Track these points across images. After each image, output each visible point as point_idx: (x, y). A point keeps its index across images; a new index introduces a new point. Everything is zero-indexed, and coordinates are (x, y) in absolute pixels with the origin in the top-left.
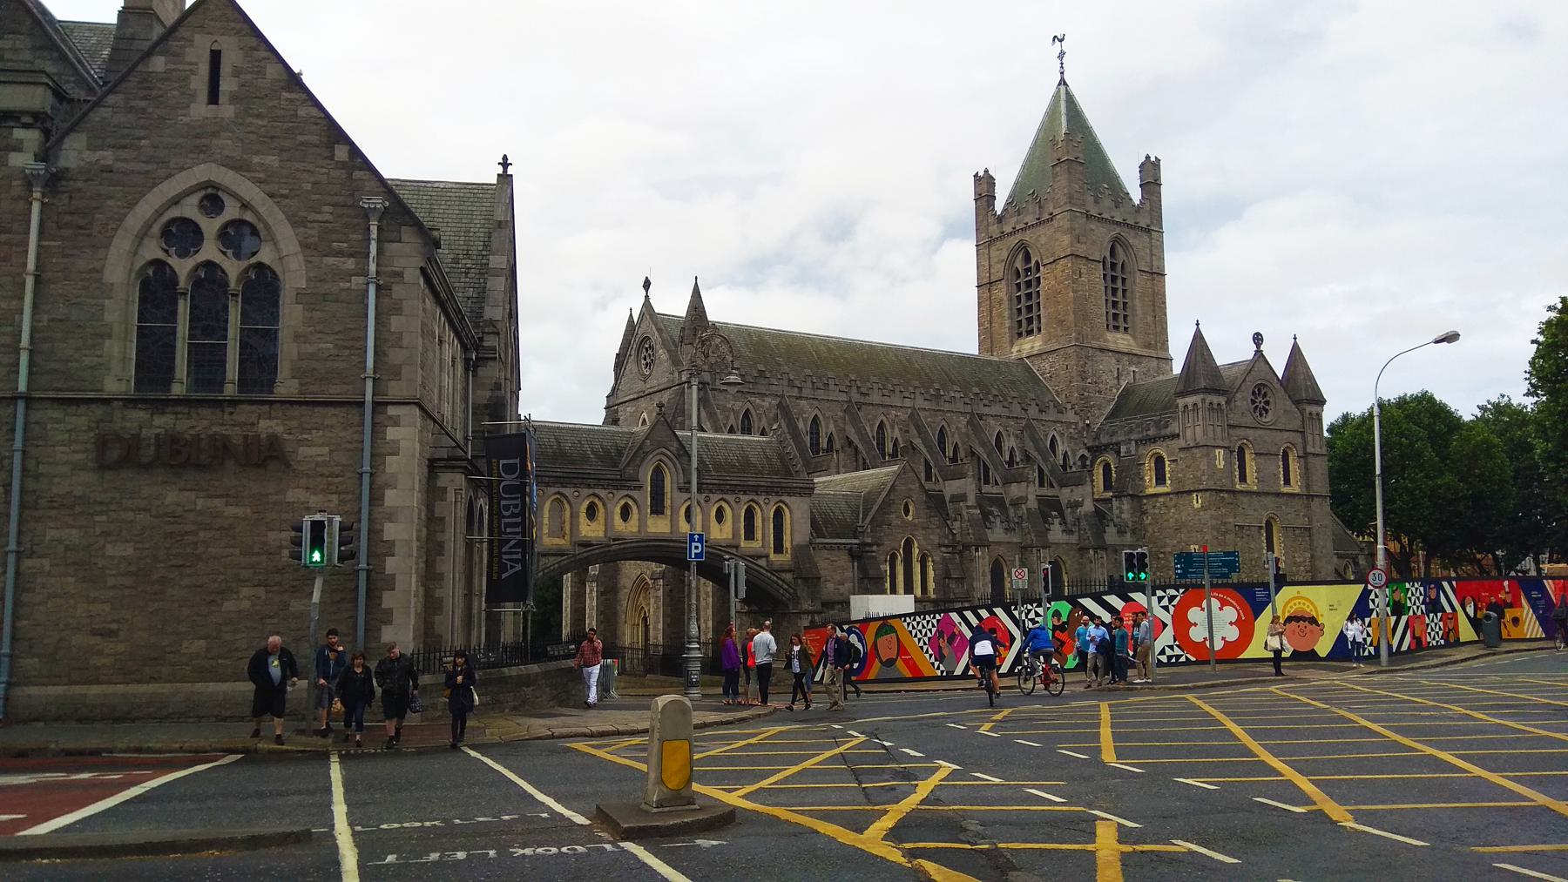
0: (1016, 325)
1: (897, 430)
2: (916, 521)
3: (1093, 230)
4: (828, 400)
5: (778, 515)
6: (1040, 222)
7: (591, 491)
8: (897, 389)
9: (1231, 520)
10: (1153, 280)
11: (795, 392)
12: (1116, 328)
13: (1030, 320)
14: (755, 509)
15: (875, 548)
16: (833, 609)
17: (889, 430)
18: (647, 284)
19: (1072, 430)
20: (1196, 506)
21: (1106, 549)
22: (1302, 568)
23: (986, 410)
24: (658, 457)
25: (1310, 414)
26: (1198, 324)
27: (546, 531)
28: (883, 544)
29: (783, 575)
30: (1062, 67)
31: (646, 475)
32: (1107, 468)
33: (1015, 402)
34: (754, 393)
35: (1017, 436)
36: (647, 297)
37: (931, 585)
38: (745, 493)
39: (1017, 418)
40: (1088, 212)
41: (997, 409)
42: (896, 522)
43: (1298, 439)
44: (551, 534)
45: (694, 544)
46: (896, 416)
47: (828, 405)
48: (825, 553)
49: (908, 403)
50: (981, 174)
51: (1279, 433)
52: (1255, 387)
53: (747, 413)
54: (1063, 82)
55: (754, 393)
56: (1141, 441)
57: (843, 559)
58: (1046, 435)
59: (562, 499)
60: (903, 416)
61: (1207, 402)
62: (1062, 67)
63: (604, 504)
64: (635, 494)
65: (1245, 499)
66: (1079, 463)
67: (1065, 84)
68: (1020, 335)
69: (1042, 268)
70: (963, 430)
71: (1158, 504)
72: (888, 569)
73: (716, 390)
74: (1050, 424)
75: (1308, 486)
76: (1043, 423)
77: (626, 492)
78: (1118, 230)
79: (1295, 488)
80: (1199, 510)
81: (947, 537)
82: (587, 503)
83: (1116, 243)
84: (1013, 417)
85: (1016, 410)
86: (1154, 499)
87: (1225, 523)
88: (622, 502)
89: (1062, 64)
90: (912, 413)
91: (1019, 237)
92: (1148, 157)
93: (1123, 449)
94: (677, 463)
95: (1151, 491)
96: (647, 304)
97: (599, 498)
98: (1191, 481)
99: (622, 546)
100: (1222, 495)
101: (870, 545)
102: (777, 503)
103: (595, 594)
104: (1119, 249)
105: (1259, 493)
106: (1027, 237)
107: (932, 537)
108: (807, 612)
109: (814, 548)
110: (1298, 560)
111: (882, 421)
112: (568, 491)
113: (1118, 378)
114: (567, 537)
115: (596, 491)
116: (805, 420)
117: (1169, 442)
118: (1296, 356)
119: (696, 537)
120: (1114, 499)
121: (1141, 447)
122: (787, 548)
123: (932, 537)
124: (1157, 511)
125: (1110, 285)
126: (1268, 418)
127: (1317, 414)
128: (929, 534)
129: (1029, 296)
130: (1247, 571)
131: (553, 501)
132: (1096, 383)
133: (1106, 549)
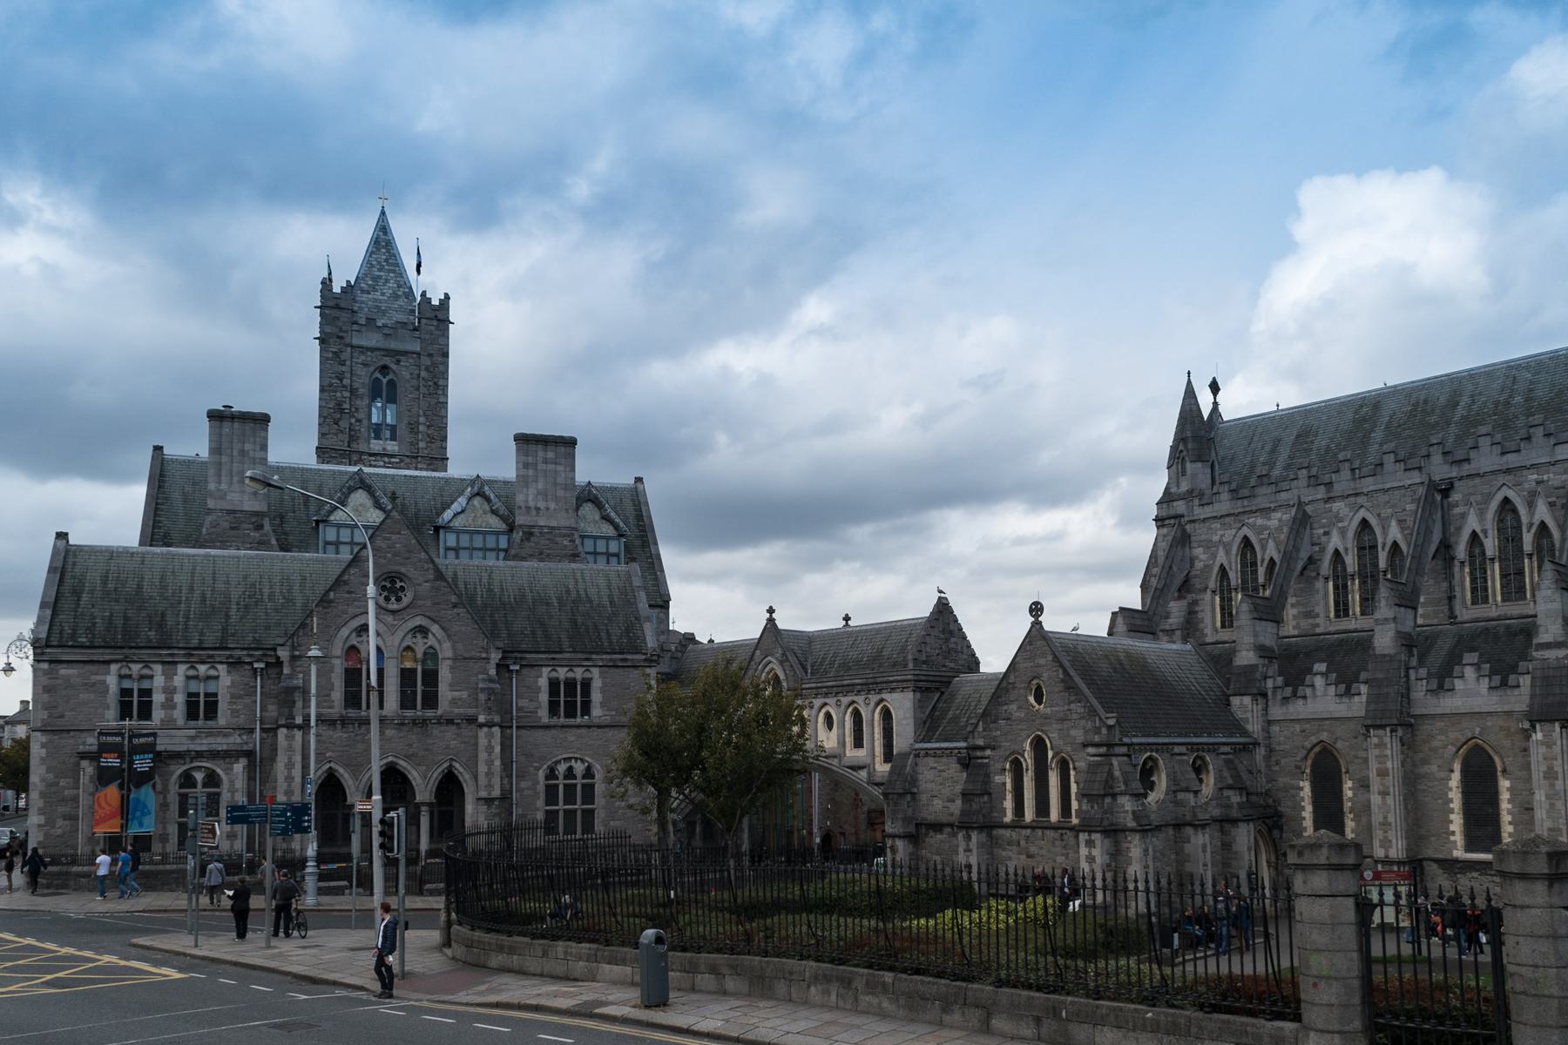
2: (1048, 710)
4: (1386, 491)
8: (1540, 431)
11: (1321, 493)
15: (988, 752)
16: (941, 832)
28: (1000, 747)
34: (1252, 512)
37: (1075, 805)
42: (1018, 714)
48: (931, 761)
53: (1246, 542)
55: (1252, 512)
57: (953, 769)
72: (1008, 781)
73: (1194, 521)
81: (1097, 731)
101: (982, 748)
107: (1073, 733)
111: (1506, 501)
116: (1343, 532)
123: (1073, 733)
128: (1068, 729)
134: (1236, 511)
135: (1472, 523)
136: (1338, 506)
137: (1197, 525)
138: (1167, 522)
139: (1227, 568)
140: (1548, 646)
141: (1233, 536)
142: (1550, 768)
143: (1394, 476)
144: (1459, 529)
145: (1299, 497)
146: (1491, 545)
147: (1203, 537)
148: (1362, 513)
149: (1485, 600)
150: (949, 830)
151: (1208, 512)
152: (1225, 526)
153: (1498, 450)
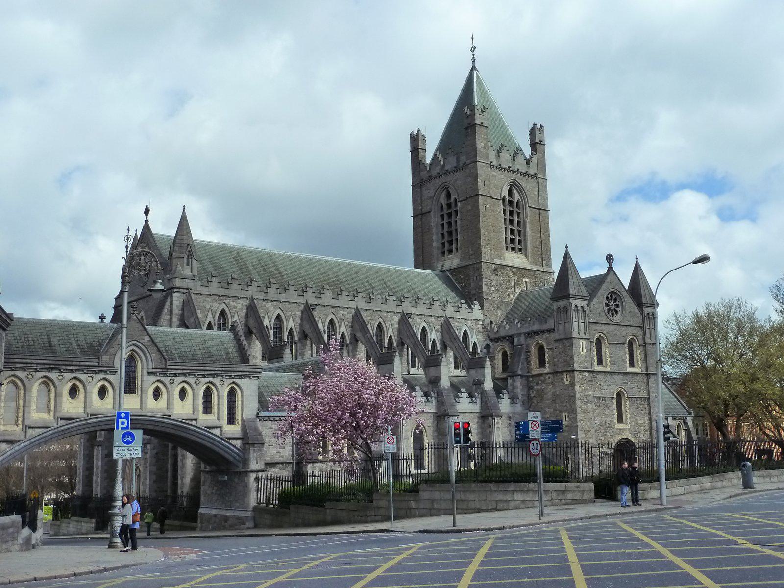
0: (441, 246)
1: (343, 326)
3: (495, 177)
5: (232, 394)
6: (457, 169)
7: (73, 375)
9: (590, 393)
11: (262, 296)
12: (513, 249)
13: (450, 243)
14: (212, 389)
16: (275, 467)
17: (337, 325)
18: (147, 211)
19: (479, 326)
20: (567, 383)
21: (501, 416)
22: (643, 428)
23: (414, 311)
24: (132, 348)
25: (648, 314)
26: (567, 247)
27: (33, 406)
29: (234, 442)
30: (473, 58)
31: (120, 364)
32: (504, 354)
33: (436, 303)
36: (147, 222)
38: (204, 376)
39: (438, 317)
40: (491, 162)
41: (421, 309)
43: (639, 332)
44: (38, 410)
45: (120, 421)
47: (288, 306)
48: (269, 424)
49: (352, 305)
50: (415, 133)
51: (625, 328)
52: (608, 294)
53: (223, 313)
56: (528, 333)
58: (460, 330)
59: (49, 382)
60: (349, 315)
61: (573, 305)
62: (473, 58)
63: (84, 386)
64: (110, 377)
65: (602, 377)
66: (485, 351)
67: (476, 69)
68: (443, 253)
69: (458, 204)
70: (396, 326)
71: (540, 382)
73: (196, 294)
74: (462, 321)
75: (647, 368)
76: (458, 320)
77: (103, 376)
78: (514, 176)
80: (568, 386)
82: (70, 384)
83: (513, 185)
86: (537, 378)
88: (100, 384)
89: (473, 55)
90: (356, 313)
91: (443, 179)
92: (535, 125)
93: (516, 340)
94: (147, 352)
95: (534, 373)
96: (146, 227)
97: (80, 381)
98: (562, 364)
99: (99, 420)
100: (584, 374)
102: (231, 384)
103: (100, 456)
105: (612, 372)
106: (449, 179)
108: (253, 471)
109: (260, 420)
110: (640, 422)
112: (54, 376)
113: (514, 287)
114: (52, 413)
115: (78, 375)
117: (547, 335)
118: (637, 272)
119: (123, 415)
120: (509, 378)
121: (528, 339)
122: (238, 420)
124: (539, 387)
125: (508, 217)
126: (617, 318)
127: (653, 314)
129: (450, 224)
130: (603, 431)
131: (41, 383)
132: (497, 289)
133: (501, 416)
134: (221, 294)
136: (269, 304)
137: (197, 296)
138: (181, 290)
139: (213, 324)
141: (218, 307)
142: (406, 435)
143: (292, 295)
145: (252, 296)
147: (201, 304)
148: (278, 311)
150: (281, 466)
151: (205, 290)
152: (213, 301)
153: (331, 296)
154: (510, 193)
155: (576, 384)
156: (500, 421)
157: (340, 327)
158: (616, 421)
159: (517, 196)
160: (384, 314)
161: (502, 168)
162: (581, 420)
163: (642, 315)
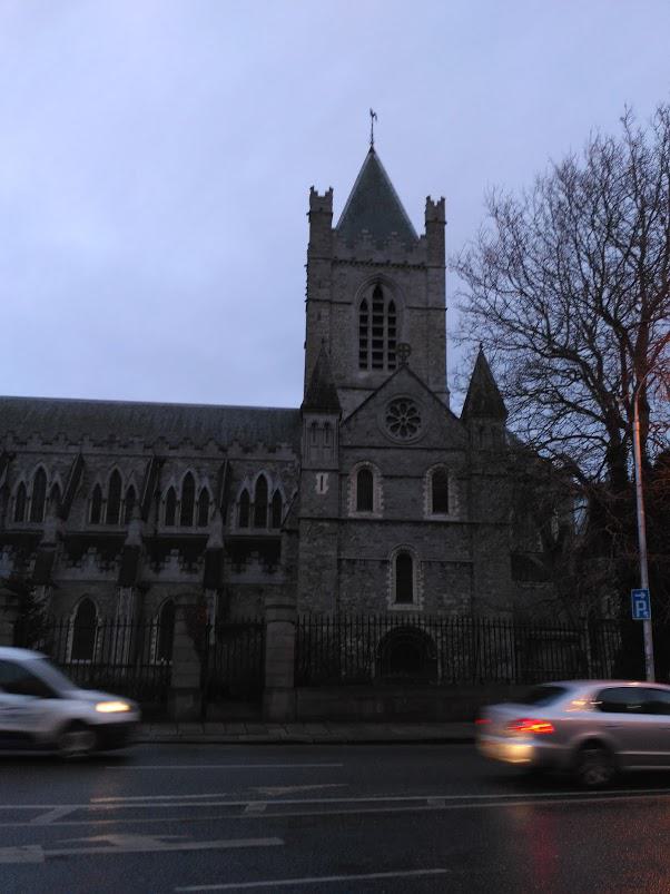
9: (330, 553)
10: (429, 315)
35: (211, 477)
46: (59, 462)
49: (73, 449)
51: (424, 453)
54: (372, 151)
58: (253, 475)
60: (67, 462)
65: (363, 529)
78: (380, 270)
79: (453, 514)
84: (205, 459)
85: (212, 450)
87: (323, 557)
100: (320, 524)
104: (386, 290)
105: (386, 520)
135: (22, 478)
140: (46, 545)
144: (15, 479)
146: (30, 491)
149: (22, 520)
154: (378, 293)
155: (303, 538)
156: (215, 596)
157: (53, 476)
158: (390, 598)
159: (388, 294)
160: (125, 459)
161: (356, 263)
162: (305, 595)
163: (469, 432)
